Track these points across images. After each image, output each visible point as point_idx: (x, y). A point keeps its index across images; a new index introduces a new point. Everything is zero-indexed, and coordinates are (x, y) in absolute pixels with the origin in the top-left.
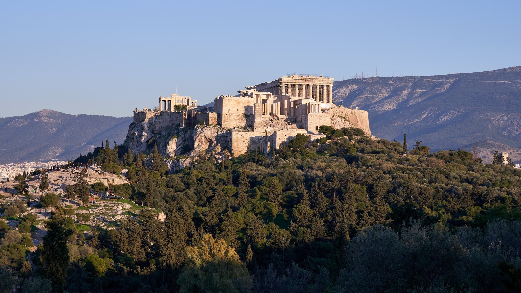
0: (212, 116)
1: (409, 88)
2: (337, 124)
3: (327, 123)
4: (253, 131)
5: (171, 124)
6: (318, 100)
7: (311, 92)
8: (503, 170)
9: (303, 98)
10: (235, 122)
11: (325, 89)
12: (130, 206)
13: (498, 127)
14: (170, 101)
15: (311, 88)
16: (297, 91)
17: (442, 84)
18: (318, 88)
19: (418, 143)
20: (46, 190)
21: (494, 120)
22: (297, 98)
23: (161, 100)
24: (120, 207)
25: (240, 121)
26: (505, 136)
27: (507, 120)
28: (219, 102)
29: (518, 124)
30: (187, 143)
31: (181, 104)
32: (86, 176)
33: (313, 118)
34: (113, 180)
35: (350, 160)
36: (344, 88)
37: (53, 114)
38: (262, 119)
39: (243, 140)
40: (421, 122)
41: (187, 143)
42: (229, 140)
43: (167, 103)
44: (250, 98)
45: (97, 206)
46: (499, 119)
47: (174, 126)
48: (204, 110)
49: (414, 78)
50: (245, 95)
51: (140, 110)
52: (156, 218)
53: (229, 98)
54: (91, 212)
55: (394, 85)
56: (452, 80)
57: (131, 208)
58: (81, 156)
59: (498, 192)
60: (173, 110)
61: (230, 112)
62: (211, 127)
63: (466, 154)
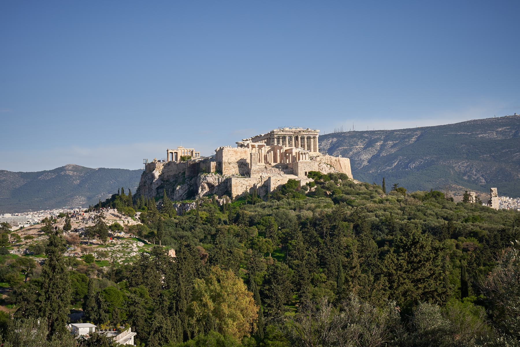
0: (213, 164)
1: (381, 140)
2: (324, 170)
4: (250, 177)
5: (178, 172)
6: (306, 149)
8: (473, 208)
9: (294, 147)
10: (234, 170)
11: (312, 140)
12: (143, 244)
13: (459, 172)
14: (177, 153)
15: (299, 139)
16: (287, 143)
17: (410, 137)
18: (306, 140)
19: (395, 185)
20: (69, 231)
21: (456, 166)
22: (288, 148)
23: (169, 152)
24: (135, 245)
26: (465, 180)
27: (467, 167)
28: (220, 153)
29: (477, 169)
30: (192, 188)
31: (186, 155)
32: (104, 218)
33: (302, 164)
34: (128, 221)
35: (336, 201)
36: (325, 141)
37: (76, 168)
38: (257, 167)
39: (241, 185)
40: (392, 169)
41: (192, 188)
42: (228, 185)
43: (174, 154)
44: (246, 149)
45: (115, 245)
46: (461, 166)
47: (180, 174)
48: (206, 161)
49: (386, 132)
50: (242, 146)
52: (166, 254)
53: (229, 148)
54: (109, 250)
55: (369, 138)
56: (419, 133)
59: (472, 227)
62: (213, 174)
63: (439, 194)
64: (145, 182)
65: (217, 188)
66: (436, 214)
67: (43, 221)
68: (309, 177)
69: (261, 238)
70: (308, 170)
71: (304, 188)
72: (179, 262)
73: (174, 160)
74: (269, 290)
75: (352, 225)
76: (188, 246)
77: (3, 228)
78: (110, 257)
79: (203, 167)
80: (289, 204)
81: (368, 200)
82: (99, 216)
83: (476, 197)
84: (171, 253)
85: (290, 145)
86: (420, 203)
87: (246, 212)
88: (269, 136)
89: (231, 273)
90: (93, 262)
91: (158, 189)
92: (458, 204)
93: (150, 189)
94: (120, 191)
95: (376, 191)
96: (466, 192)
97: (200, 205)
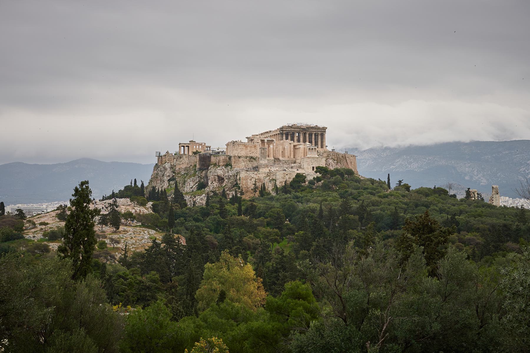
3: (323, 164)
7: (307, 139)
9: (301, 143)
10: (243, 164)
11: (319, 137)
14: (188, 146)
15: (307, 136)
19: (400, 182)
22: (296, 143)
23: (181, 145)
25: (248, 162)
30: (203, 180)
33: (310, 160)
34: (140, 210)
51: (163, 154)
54: (121, 237)
57: (155, 234)
58: (113, 193)
60: (190, 154)
61: (239, 155)
64: (157, 174)
65: (226, 180)
66: (439, 209)
67: (58, 209)
68: (316, 172)
69: (269, 229)
70: (316, 165)
71: (311, 182)
72: (189, 250)
73: (186, 153)
74: (276, 277)
75: (357, 217)
76: (198, 235)
77: (19, 215)
78: (122, 244)
79: (213, 159)
80: (297, 197)
81: (373, 194)
82: (113, 205)
83: (478, 194)
84: (182, 241)
85: (299, 141)
86: (424, 199)
87: (254, 203)
88: (279, 132)
89: (240, 260)
90: (107, 247)
91: (169, 180)
92: (462, 200)
93: (162, 181)
94: (133, 183)
95: (381, 187)
96: (469, 189)
97: (211, 197)
